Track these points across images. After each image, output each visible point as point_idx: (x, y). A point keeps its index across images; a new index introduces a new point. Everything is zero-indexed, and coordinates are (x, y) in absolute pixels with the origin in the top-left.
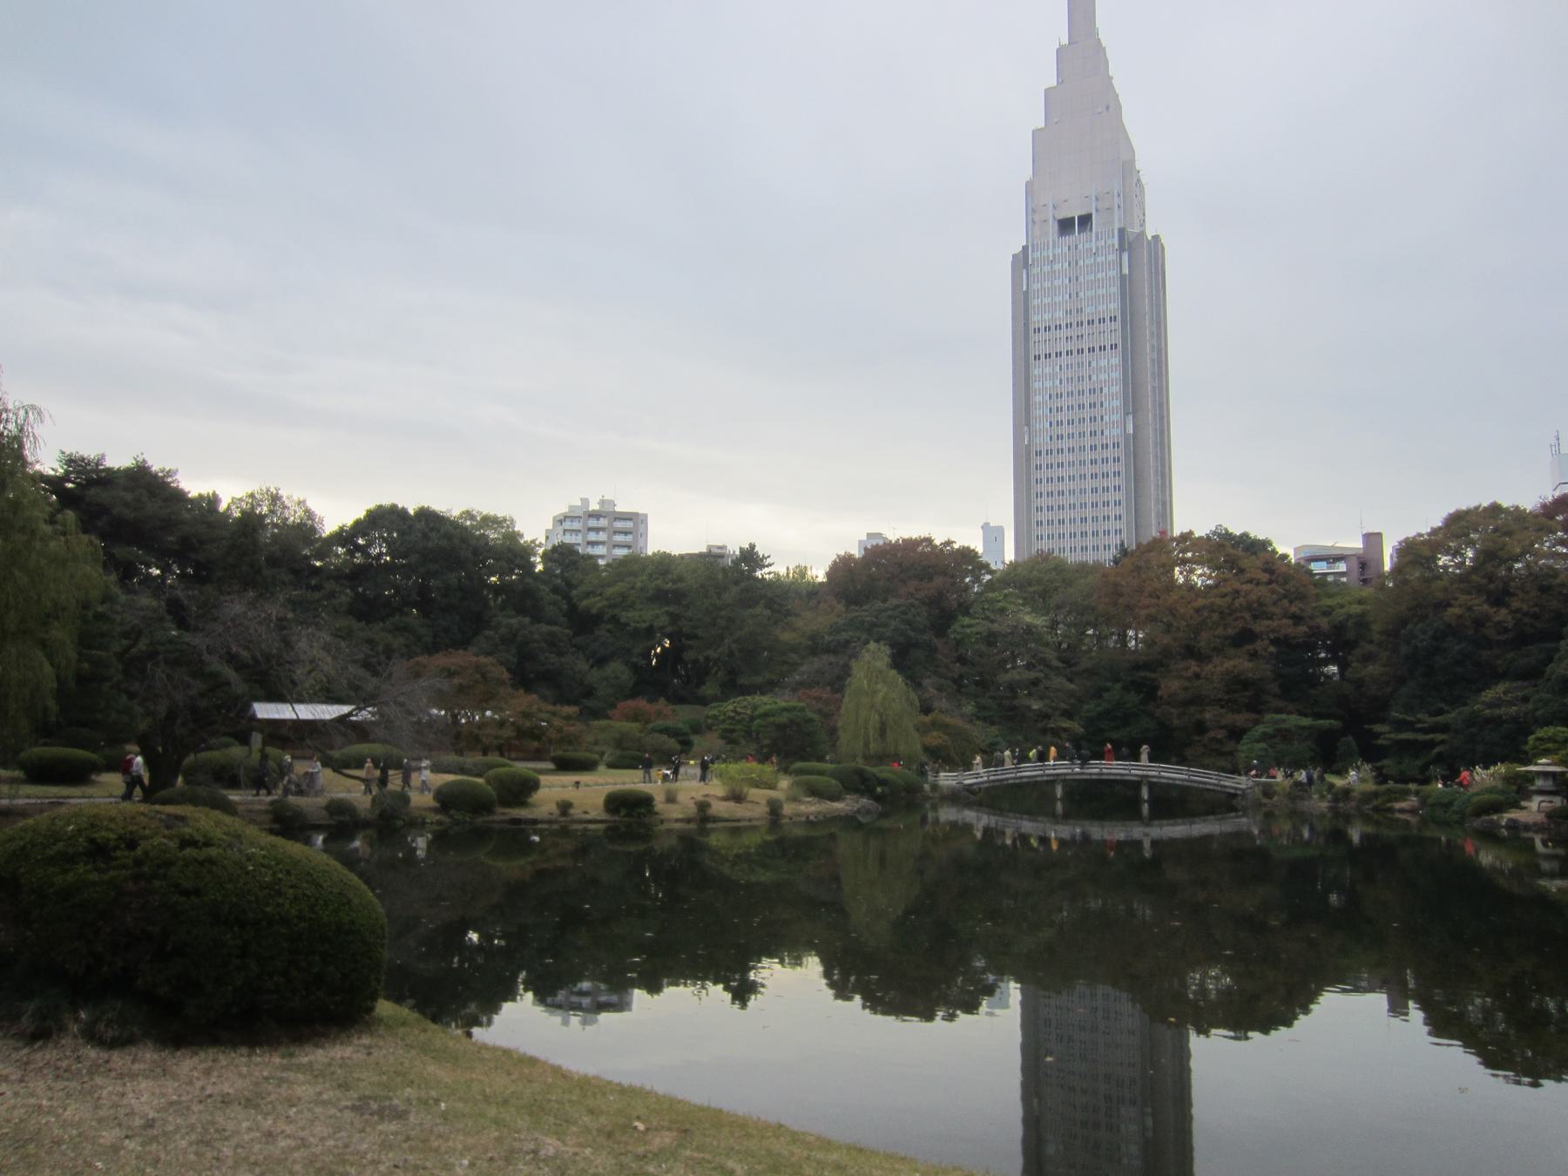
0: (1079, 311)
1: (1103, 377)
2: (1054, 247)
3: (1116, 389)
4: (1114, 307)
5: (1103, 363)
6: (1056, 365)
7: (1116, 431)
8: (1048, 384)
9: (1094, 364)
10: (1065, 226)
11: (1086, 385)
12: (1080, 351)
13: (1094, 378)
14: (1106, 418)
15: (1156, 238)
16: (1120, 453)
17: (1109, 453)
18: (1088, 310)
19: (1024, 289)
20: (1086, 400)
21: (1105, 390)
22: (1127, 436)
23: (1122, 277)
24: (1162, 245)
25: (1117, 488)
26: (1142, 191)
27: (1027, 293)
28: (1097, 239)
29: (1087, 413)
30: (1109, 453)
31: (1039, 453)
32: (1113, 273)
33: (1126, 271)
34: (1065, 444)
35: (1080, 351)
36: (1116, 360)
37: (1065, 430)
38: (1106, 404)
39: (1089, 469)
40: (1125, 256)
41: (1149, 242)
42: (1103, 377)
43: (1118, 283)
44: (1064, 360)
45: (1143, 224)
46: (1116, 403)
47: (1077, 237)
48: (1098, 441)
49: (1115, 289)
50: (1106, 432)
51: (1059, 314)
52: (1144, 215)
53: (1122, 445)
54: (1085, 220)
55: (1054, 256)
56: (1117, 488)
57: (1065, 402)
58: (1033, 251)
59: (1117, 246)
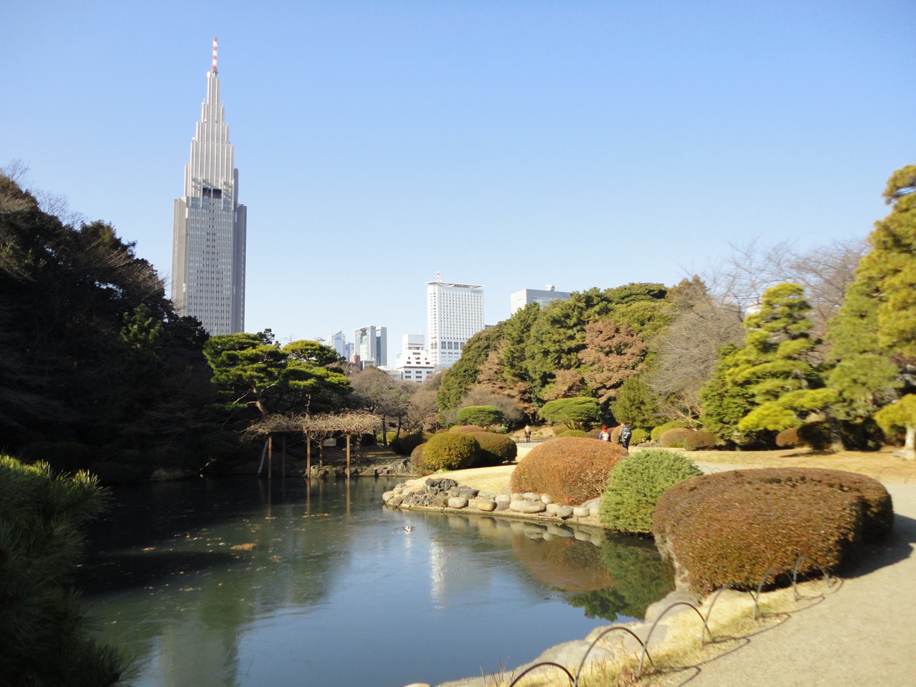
1: (223, 267)
3: (230, 273)
4: (231, 236)
5: (224, 260)
7: (229, 292)
8: (197, 265)
9: (219, 260)
10: (206, 191)
11: (215, 270)
13: (219, 266)
14: (224, 286)
16: (230, 302)
17: (225, 302)
19: (187, 216)
21: (224, 273)
25: (228, 318)
32: (231, 221)
34: (204, 294)
36: (230, 261)
37: (204, 288)
38: (224, 279)
40: (236, 214)
42: (223, 267)
43: (232, 225)
44: (205, 256)
46: (230, 280)
48: (219, 295)
49: (231, 228)
50: (224, 292)
51: (204, 233)
54: (217, 193)
56: (228, 318)
59: (233, 209)
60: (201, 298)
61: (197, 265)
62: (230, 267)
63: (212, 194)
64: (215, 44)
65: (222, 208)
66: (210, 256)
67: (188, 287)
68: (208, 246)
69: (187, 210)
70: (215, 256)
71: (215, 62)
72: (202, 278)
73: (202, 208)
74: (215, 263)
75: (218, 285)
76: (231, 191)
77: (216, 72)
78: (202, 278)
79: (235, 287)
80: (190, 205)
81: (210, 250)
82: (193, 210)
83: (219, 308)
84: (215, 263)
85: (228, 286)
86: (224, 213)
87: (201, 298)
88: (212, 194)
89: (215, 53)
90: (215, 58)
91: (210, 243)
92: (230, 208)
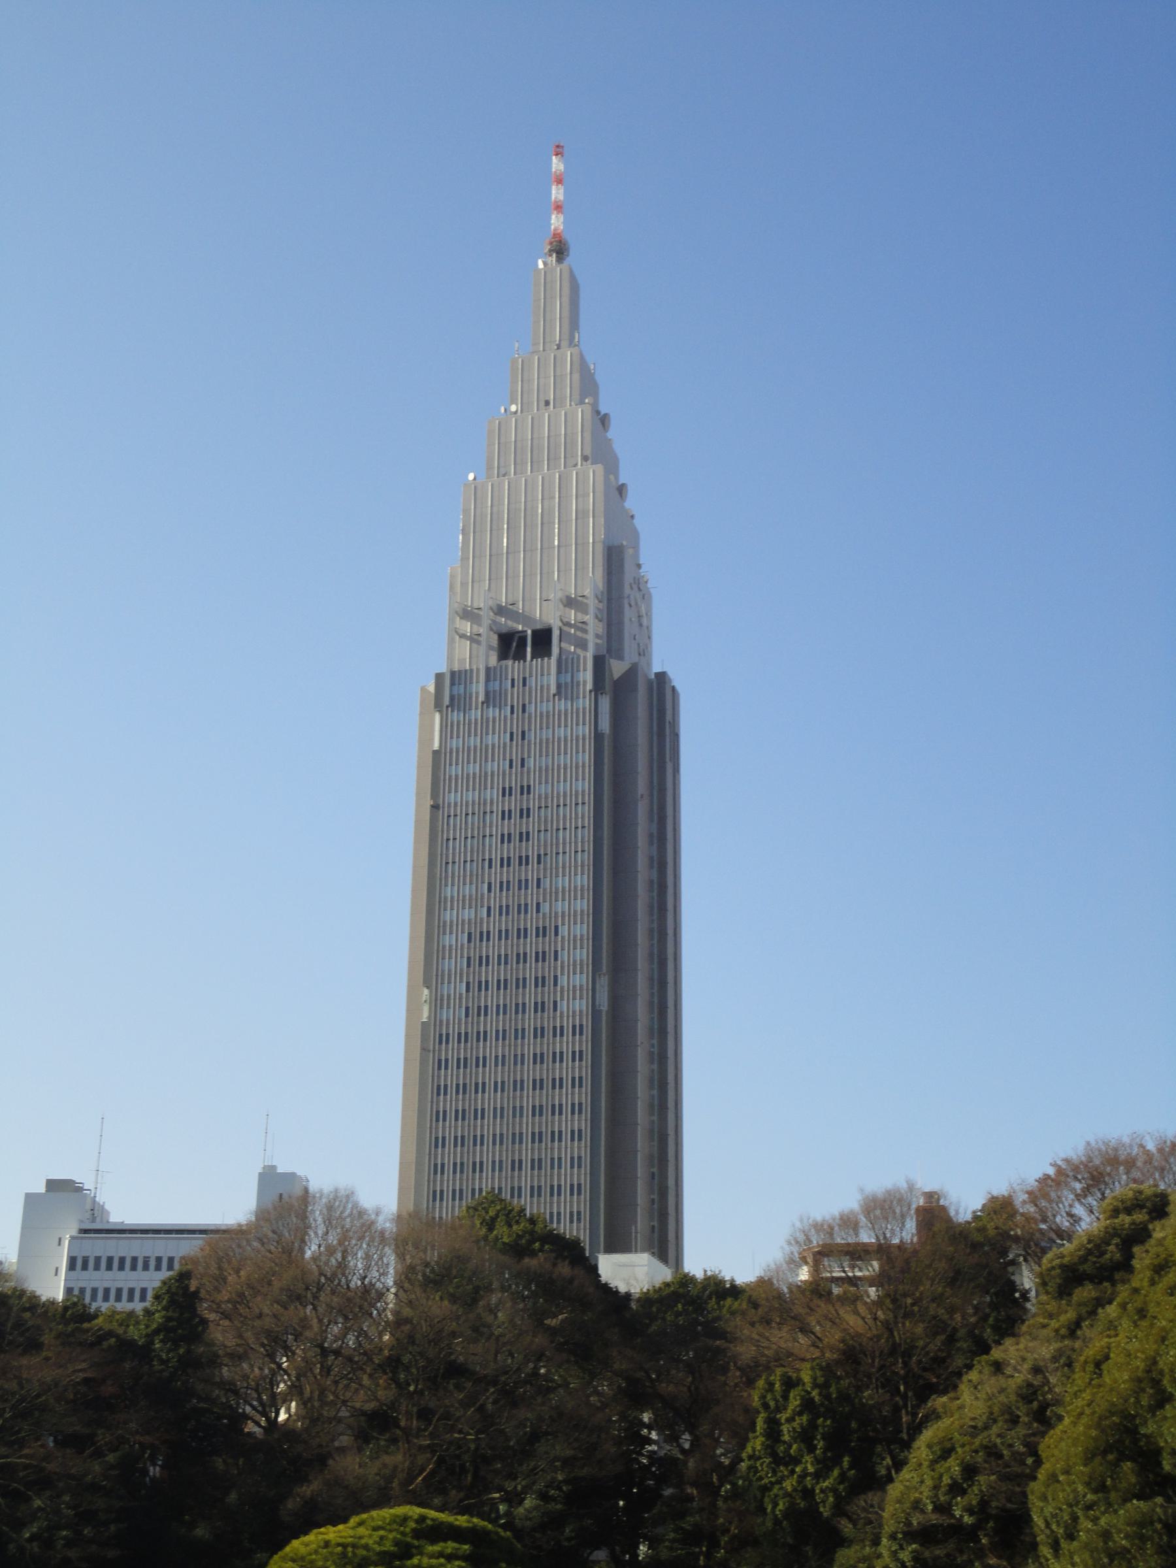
0: (526, 790)
2: (488, 680)
3: (582, 929)
4: (585, 785)
6: (483, 882)
7: (581, 1005)
8: (467, 914)
11: (531, 921)
12: (524, 861)
13: (546, 908)
14: (563, 981)
15: (662, 677)
17: (565, 1044)
18: (539, 789)
19: (436, 746)
20: (531, 945)
21: (564, 931)
22: (596, 1013)
23: (598, 737)
24: (673, 688)
26: (646, 597)
27: (436, 753)
28: (559, 672)
29: (530, 970)
30: (565, 1044)
31: (443, 1039)
32: (585, 730)
33: (605, 725)
35: (524, 861)
36: (583, 880)
39: (529, 1072)
40: (605, 703)
41: (650, 683)
43: (589, 746)
44: (497, 875)
45: (644, 652)
46: (583, 954)
47: (531, 663)
49: (586, 757)
50: (563, 1006)
51: (492, 794)
52: (649, 638)
53: (587, 1031)
54: (542, 639)
55: (487, 694)
57: (493, 949)
58: (452, 684)
59: (589, 686)
60: (482, 1036)
61: (467, 914)
62: (583, 905)
63: (529, 649)
64: (557, 164)
65: (553, 690)
66: (513, 874)
67: (437, 1003)
68: (506, 838)
69: (437, 717)
70: (531, 872)
71: (556, 221)
72: (484, 961)
73: (486, 702)
74: (531, 896)
75: (540, 982)
76: (594, 629)
77: (560, 249)
78: (484, 961)
79: (604, 982)
80: (447, 701)
81: (512, 850)
82: (455, 716)
83: (539, 1072)
84: (531, 896)
85: (581, 979)
86: (562, 705)
87: (482, 1036)
88: (529, 649)
89: (557, 193)
90: (558, 208)
91: (513, 826)
92: (574, 684)
